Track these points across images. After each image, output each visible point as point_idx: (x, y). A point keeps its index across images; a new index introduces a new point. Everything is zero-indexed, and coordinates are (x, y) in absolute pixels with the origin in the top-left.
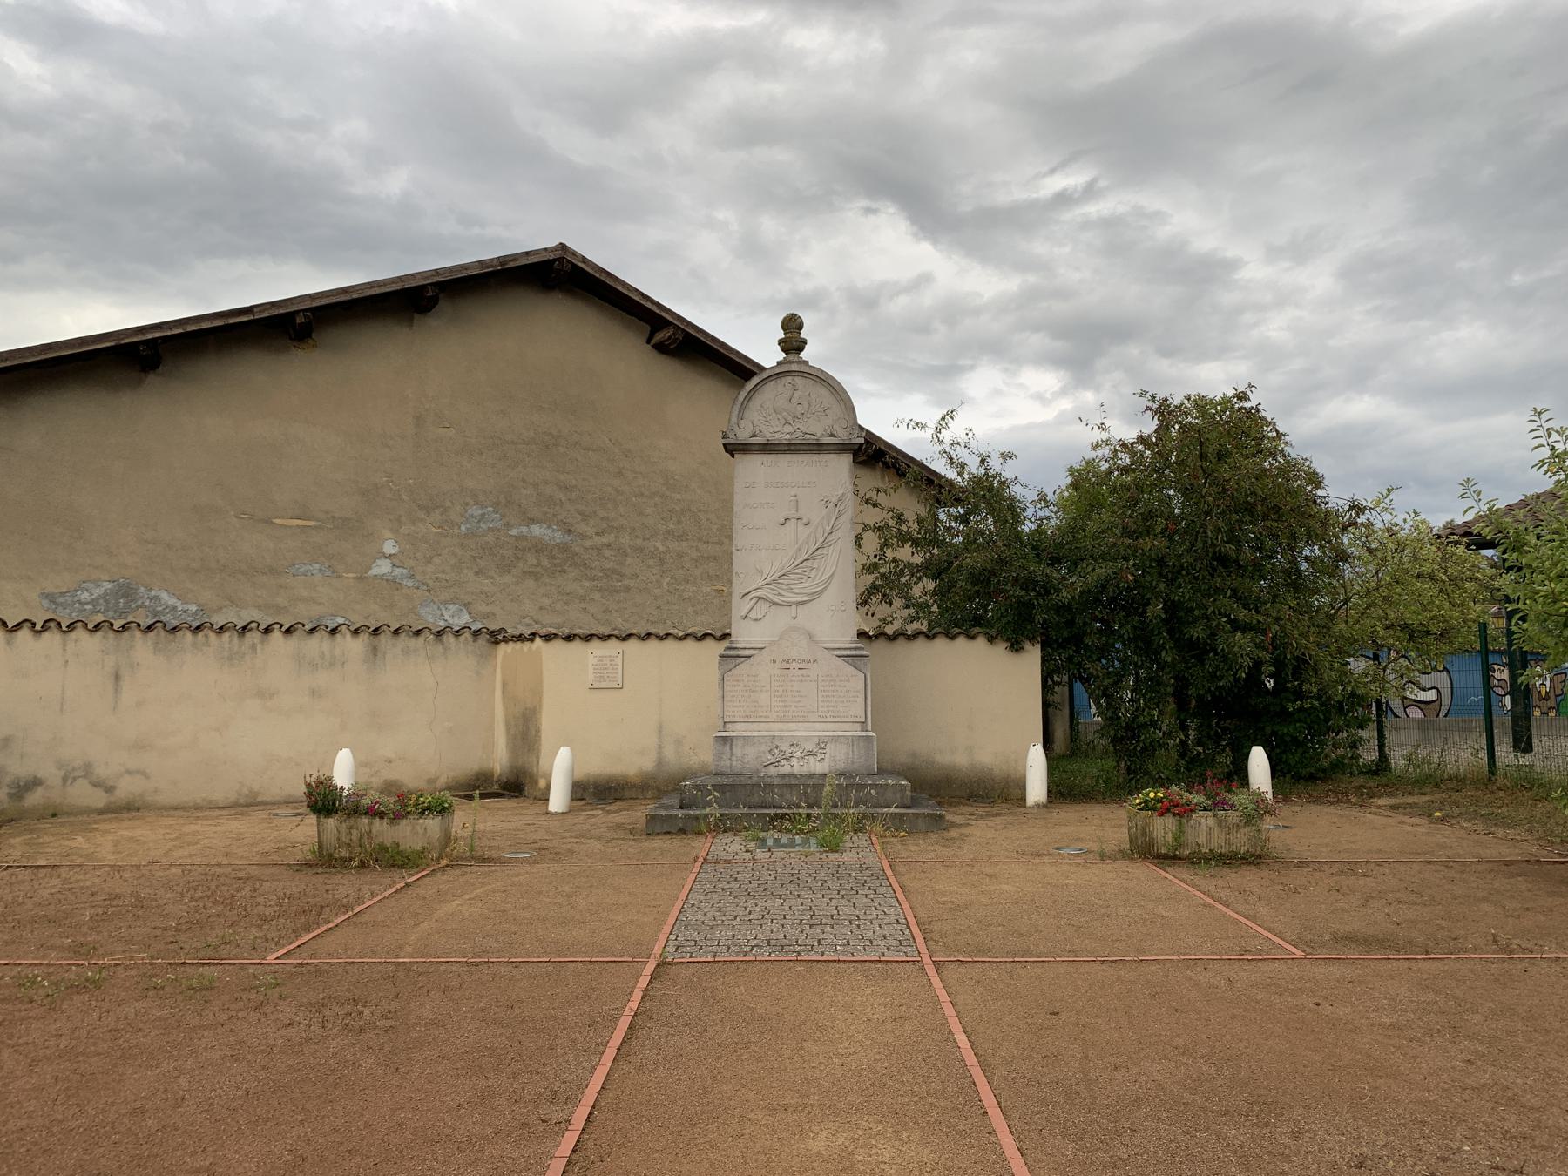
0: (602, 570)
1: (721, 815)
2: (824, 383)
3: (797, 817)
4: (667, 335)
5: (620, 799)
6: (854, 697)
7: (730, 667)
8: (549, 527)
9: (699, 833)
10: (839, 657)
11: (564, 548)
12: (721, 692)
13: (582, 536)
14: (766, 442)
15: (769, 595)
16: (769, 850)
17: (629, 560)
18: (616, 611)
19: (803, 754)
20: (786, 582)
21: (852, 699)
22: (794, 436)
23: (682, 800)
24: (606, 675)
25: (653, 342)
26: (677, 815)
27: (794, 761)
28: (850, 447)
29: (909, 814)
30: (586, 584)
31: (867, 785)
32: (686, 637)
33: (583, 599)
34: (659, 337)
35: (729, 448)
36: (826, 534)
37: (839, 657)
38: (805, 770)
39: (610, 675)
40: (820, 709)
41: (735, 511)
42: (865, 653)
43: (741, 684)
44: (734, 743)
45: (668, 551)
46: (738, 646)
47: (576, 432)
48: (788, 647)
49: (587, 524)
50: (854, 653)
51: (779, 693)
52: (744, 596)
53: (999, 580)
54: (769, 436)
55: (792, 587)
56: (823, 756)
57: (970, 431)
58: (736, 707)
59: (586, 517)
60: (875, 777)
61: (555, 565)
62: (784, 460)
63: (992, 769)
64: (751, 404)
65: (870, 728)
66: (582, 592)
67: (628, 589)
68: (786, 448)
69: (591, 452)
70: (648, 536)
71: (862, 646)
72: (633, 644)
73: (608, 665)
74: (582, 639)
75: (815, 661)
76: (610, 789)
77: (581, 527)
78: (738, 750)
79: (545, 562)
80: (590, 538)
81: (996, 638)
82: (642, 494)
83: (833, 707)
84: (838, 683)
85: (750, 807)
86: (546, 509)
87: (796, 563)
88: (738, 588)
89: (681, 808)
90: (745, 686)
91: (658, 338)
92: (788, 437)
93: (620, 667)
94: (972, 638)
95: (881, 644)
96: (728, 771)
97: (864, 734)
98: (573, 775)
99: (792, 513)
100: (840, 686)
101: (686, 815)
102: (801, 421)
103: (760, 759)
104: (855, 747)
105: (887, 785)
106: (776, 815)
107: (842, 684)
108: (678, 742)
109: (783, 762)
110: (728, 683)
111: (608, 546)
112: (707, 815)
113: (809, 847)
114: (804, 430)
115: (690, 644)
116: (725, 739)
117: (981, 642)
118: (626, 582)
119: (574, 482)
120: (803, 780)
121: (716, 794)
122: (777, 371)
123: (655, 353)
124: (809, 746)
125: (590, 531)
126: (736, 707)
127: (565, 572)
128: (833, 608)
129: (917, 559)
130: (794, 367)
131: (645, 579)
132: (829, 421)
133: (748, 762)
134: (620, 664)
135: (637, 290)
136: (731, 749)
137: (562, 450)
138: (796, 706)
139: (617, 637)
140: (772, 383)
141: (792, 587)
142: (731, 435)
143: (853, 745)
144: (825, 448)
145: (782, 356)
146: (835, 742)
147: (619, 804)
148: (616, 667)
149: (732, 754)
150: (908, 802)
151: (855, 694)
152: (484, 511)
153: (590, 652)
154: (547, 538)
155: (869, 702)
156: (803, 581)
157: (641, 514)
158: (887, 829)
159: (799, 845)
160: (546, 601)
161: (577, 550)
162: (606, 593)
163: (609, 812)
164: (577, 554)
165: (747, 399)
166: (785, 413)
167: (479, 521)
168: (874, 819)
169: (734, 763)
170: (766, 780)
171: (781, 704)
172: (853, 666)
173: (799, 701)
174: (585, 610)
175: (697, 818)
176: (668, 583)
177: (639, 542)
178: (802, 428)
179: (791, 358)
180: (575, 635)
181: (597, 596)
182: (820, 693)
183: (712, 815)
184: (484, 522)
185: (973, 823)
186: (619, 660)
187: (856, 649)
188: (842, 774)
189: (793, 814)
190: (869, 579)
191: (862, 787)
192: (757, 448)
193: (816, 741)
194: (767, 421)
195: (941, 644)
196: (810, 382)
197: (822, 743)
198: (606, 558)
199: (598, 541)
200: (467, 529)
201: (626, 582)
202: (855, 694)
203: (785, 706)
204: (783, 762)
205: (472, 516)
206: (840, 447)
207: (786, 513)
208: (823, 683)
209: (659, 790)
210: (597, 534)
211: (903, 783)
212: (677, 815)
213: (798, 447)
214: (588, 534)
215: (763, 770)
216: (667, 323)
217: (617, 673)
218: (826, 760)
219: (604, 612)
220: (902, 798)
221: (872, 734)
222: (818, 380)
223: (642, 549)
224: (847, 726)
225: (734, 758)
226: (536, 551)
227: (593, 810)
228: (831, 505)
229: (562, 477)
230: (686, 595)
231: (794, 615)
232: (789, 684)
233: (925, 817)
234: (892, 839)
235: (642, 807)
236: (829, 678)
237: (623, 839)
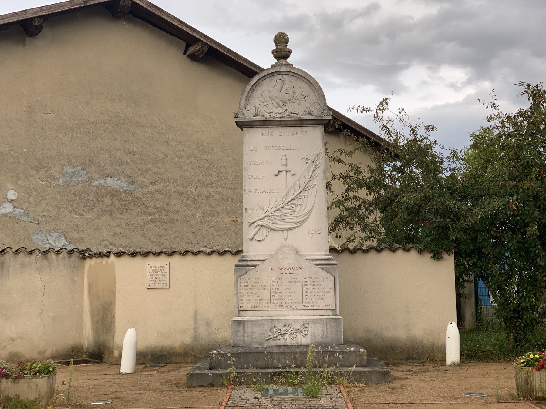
0: (155, 208)
1: (238, 373)
2: (303, 79)
3: (290, 374)
4: (197, 48)
5: (169, 363)
6: (326, 292)
7: (243, 274)
8: (119, 179)
9: (223, 386)
10: (317, 265)
11: (130, 193)
12: (236, 290)
13: (141, 185)
14: (264, 119)
15: (268, 224)
16: (271, 397)
17: (173, 201)
18: (165, 236)
19: (293, 332)
20: (279, 214)
21: (326, 294)
22: (284, 115)
23: (210, 364)
24: (158, 280)
25: (188, 53)
26: (208, 374)
27: (287, 336)
28: (322, 122)
29: (365, 371)
30: (144, 217)
31: (336, 352)
32: (212, 253)
33: (142, 228)
34: (192, 49)
35: (240, 124)
36: (306, 182)
37: (317, 265)
38: (294, 342)
40: (304, 301)
41: (244, 167)
42: (334, 262)
43: (250, 285)
44: (246, 325)
45: (199, 194)
46: (247, 258)
47: (136, 115)
48: (282, 259)
49: (145, 177)
50: (327, 262)
51: (276, 291)
52: (250, 225)
53: (425, 211)
54: (266, 115)
55: (284, 218)
56: (306, 333)
57: (403, 110)
58: (246, 300)
59: (144, 173)
60: (343, 346)
61: (124, 205)
62: (277, 132)
63: (422, 340)
64: (254, 94)
65: (338, 313)
66: (142, 223)
67: (172, 221)
68: (278, 123)
69: (146, 129)
70: (186, 184)
71: (333, 257)
72: (176, 259)
73: (160, 272)
74: (141, 255)
75: (300, 268)
76: (162, 356)
77: (140, 180)
78: (248, 330)
79: (117, 203)
80: (146, 186)
81: (424, 251)
82: (181, 156)
83: (313, 299)
84: (316, 283)
85: (257, 368)
86: (116, 167)
87: (286, 202)
88: (247, 219)
89: (210, 369)
90: (252, 286)
91: (191, 51)
92: (279, 115)
93: (168, 274)
94: (408, 250)
95: (346, 256)
96: (242, 343)
97: (334, 317)
98: (137, 348)
99: (284, 168)
100: (317, 285)
101: (213, 374)
102: (288, 105)
103: (263, 336)
104: (328, 326)
105: (350, 351)
106: (275, 373)
107: (319, 284)
108: (208, 324)
109: (280, 337)
110: (241, 284)
111: (159, 192)
112: (227, 374)
113: (298, 395)
114: (291, 110)
115: (215, 258)
116: (239, 322)
117: (413, 253)
118: (171, 216)
120: (293, 349)
121: (234, 359)
122: (271, 71)
123: (189, 60)
124: (297, 326)
125: (147, 182)
126: (246, 300)
127: (130, 209)
128: (312, 232)
129: (370, 198)
130: (283, 69)
131: (184, 214)
132: (306, 105)
133: (255, 338)
134: (168, 272)
135: (176, 18)
136: (244, 328)
137: (127, 127)
138: (288, 299)
139: (166, 254)
140: (268, 80)
141: (284, 218)
142: (241, 115)
143: (327, 325)
144: (305, 123)
145: (274, 61)
146: (315, 323)
147: (168, 367)
148: (165, 274)
149: (244, 332)
150: (365, 363)
151: (328, 290)
152: (75, 169)
153: (147, 263)
154: (118, 187)
155: (337, 296)
156: (292, 213)
157: (181, 169)
158: (351, 381)
159: (290, 393)
160: (118, 230)
161: (138, 194)
162: (158, 224)
163: (162, 372)
164: (138, 198)
165: (251, 91)
166: (277, 100)
167: (71, 177)
168: (342, 375)
169: (246, 338)
170: (268, 349)
171: (277, 298)
172: (327, 272)
173: (290, 296)
174: (144, 235)
175: (221, 375)
176: (200, 216)
177: (180, 189)
178: (289, 110)
179: (281, 62)
180: (137, 253)
181: (152, 225)
182: (304, 290)
183: (231, 373)
184: (76, 177)
185: (410, 377)
186: (167, 270)
187: (328, 259)
188: (319, 345)
189: (287, 372)
190: (337, 212)
191: (332, 353)
192: (258, 123)
193: (301, 322)
194: (265, 105)
195: (386, 255)
196: (295, 79)
197: (306, 324)
198: (158, 200)
199: (152, 188)
200: (64, 181)
201: (171, 216)
202: (328, 290)
203: (281, 299)
204: (280, 337)
205: (67, 173)
206: (316, 122)
207: (280, 168)
208: (306, 283)
209: (195, 357)
210: (152, 184)
211: (361, 350)
212: (208, 374)
213: (287, 123)
214: (145, 184)
215: (266, 342)
216: (197, 41)
217: (166, 278)
218: (309, 335)
219: (156, 237)
220: (361, 360)
221: (339, 317)
222: (299, 77)
223: (181, 194)
224: (322, 312)
225: (246, 335)
226: (111, 196)
227: (150, 371)
228: (310, 162)
229: (127, 146)
230: (212, 224)
231: (285, 237)
232: (283, 284)
233: (377, 374)
234: (355, 389)
235: (185, 369)
236: (310, 280)
237: (171, 391)
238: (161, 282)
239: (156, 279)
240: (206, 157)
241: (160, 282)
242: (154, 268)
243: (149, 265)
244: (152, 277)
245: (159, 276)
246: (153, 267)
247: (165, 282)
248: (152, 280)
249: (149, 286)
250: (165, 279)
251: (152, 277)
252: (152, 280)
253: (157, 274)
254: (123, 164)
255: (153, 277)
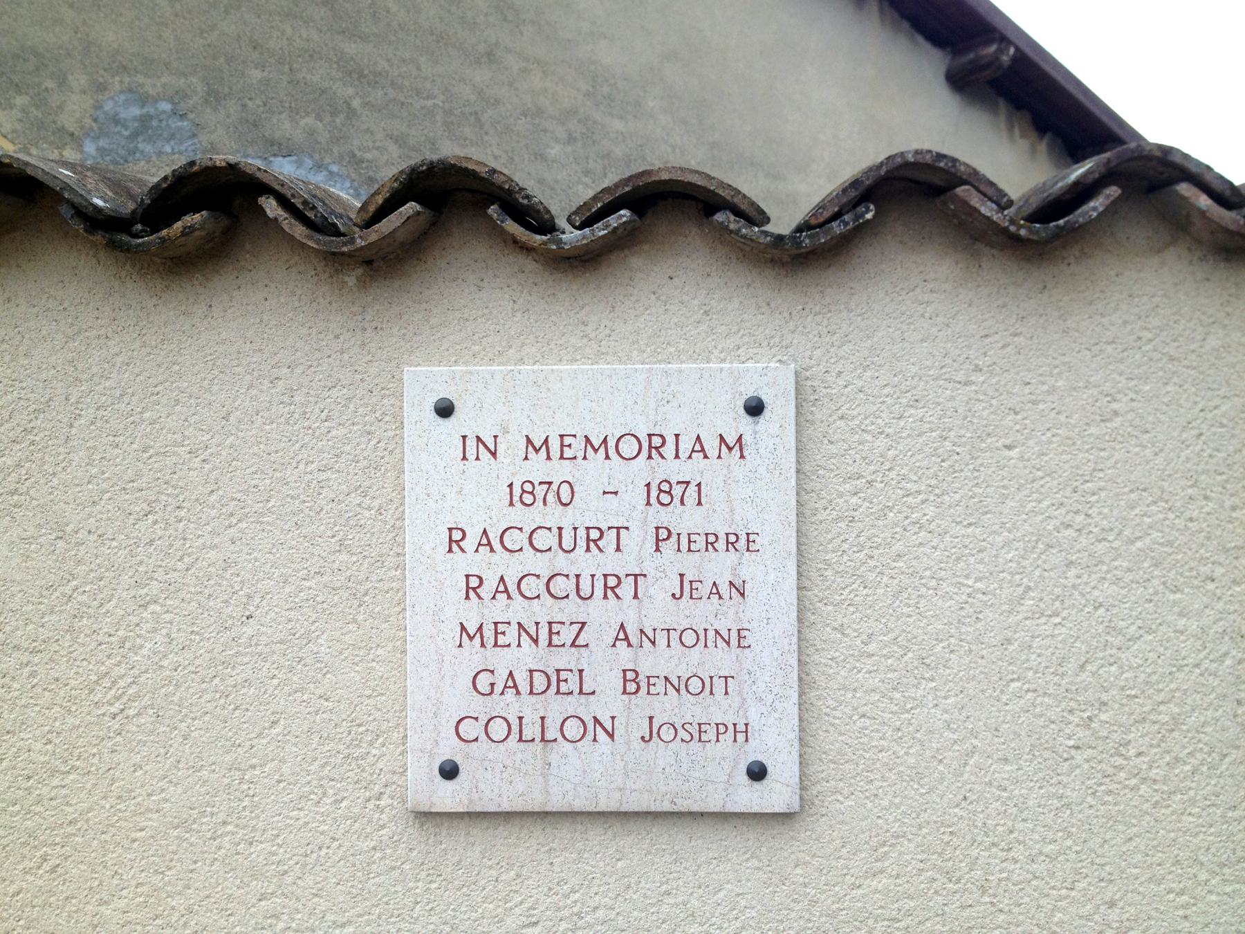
8: (319, 166)
39: (651, 662)
73: (638, 541)
82: (540, 112)
119: (382, 65)
148: (718, 567)
152: (148, 109)
167: (135, 135)
184: (149, 140)
200: (101, 150)
205: (116, 120)
217: (739, 639)
229: (351, 48)
238: (667, 707)
239: (564, 659)
240: (618, 125)
241: (643, 705)
242: (538, 469)
243: (445, 410)
244: (499, 610)
245: (626, 611)
246: (511, 447)
247: (719, 710)
248: (502, 661)
249: (449, 772)
250: (720, 660)
251: (499, 610)
252: (502, 661)
253: (586, 563)
254: (334, 114)
255: (517, 610)
